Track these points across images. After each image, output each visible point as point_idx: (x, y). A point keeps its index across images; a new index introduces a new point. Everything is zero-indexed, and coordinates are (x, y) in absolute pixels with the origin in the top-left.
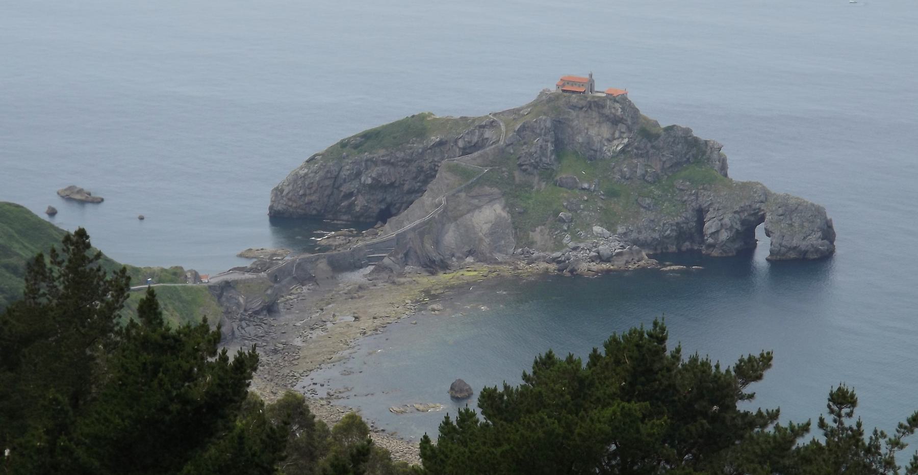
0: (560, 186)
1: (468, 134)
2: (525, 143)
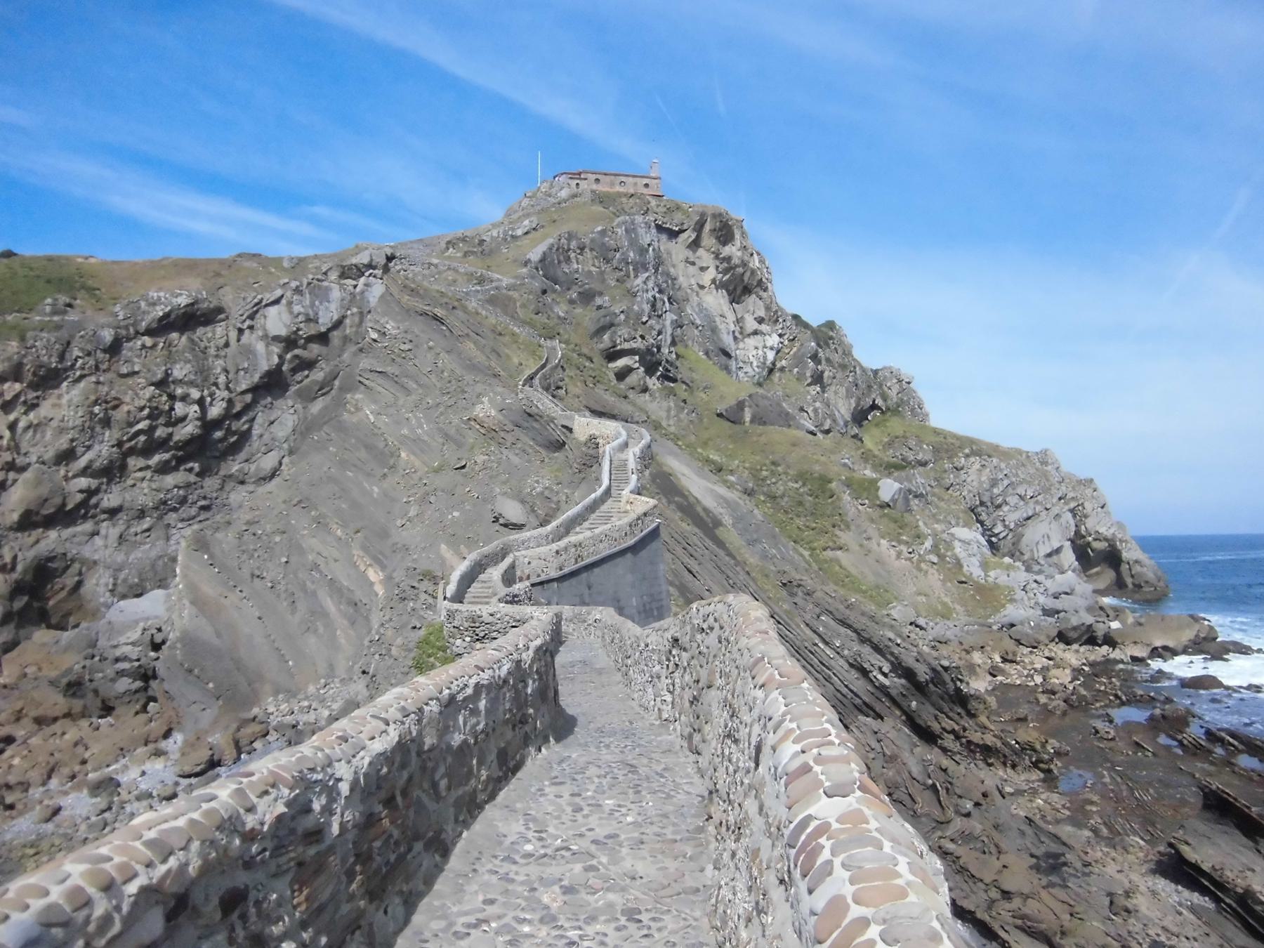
0: (758, 420)
1: (297, 290)
2: (587, 297)
